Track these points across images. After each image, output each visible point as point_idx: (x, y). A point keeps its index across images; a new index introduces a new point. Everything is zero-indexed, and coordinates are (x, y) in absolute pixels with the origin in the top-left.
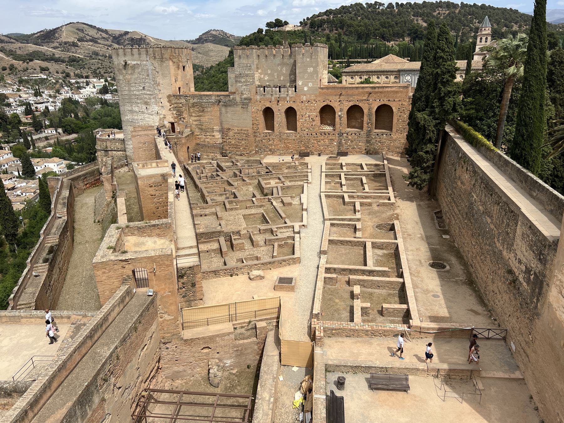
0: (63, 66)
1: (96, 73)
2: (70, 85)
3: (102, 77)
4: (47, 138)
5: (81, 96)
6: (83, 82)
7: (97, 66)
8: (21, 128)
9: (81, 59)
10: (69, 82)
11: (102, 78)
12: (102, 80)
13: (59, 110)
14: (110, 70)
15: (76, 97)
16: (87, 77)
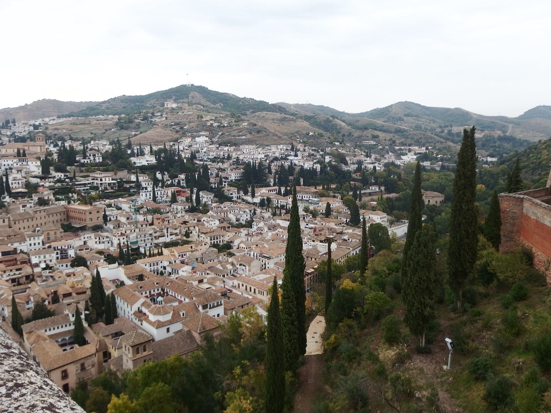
0: (388, 136)
1: (419, 142)
2: (394, 151)
3: (424, 145)
4: (370, 194)
5: (402, 161)
6: (406, 150)
7: (419, 136)
8: (352, 182)
9: (406, 131)
10: (394, 149)
11: (423, 147)
12: (424, 148)
13: (384, 170)
14: (430, 140)
15: (398, 162)
16: (410, 145)
